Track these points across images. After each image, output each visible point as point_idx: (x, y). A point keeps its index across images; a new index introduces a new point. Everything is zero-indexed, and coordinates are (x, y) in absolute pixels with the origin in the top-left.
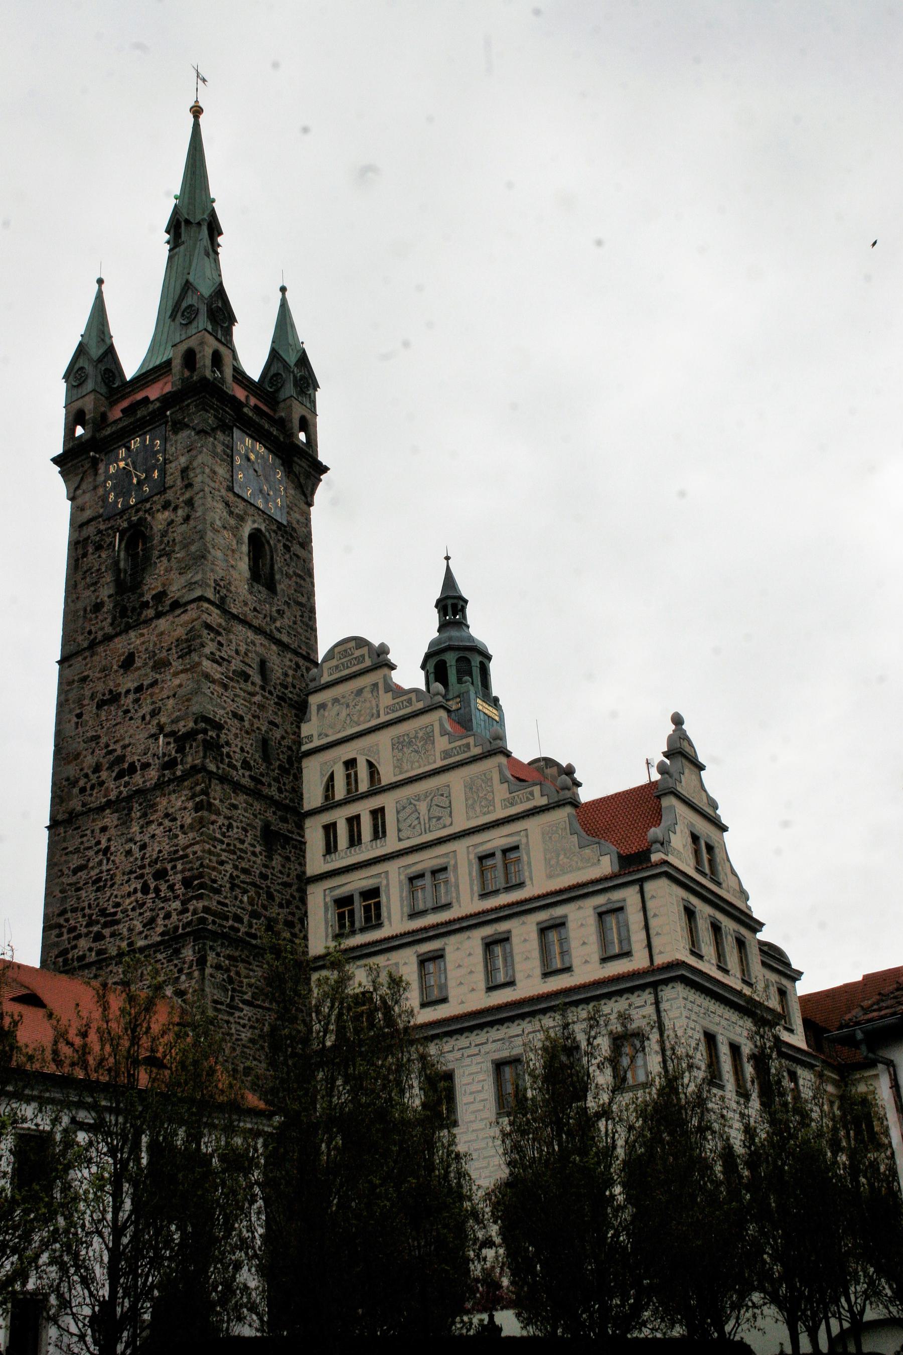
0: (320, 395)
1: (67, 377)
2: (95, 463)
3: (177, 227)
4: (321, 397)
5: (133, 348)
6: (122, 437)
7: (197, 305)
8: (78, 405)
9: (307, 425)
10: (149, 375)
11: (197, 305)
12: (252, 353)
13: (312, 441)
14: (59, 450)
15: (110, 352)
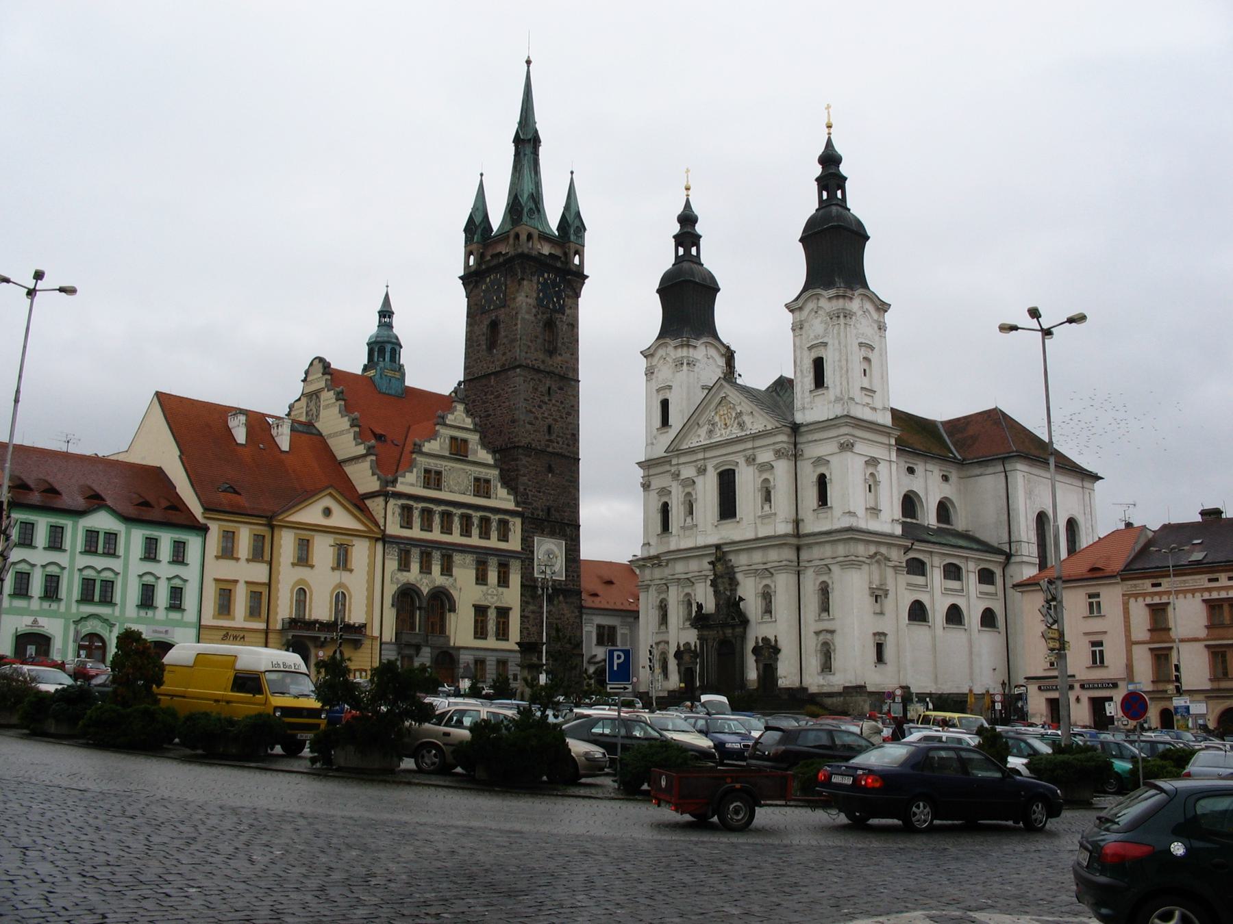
0: (586, 234)
1: (466, 230)
2: (477, 282)
3: (517, 140)
4: (588, 236)
5: (496, 218)
6: (489, 270)
7: (524, 203)
8: (469, 248)
9: (580, 252)
10: (503, 236)
11: (524, 203)
12: (553, 215)
13: (582, 261)
14: (462, 273)
15: (486, 216)
